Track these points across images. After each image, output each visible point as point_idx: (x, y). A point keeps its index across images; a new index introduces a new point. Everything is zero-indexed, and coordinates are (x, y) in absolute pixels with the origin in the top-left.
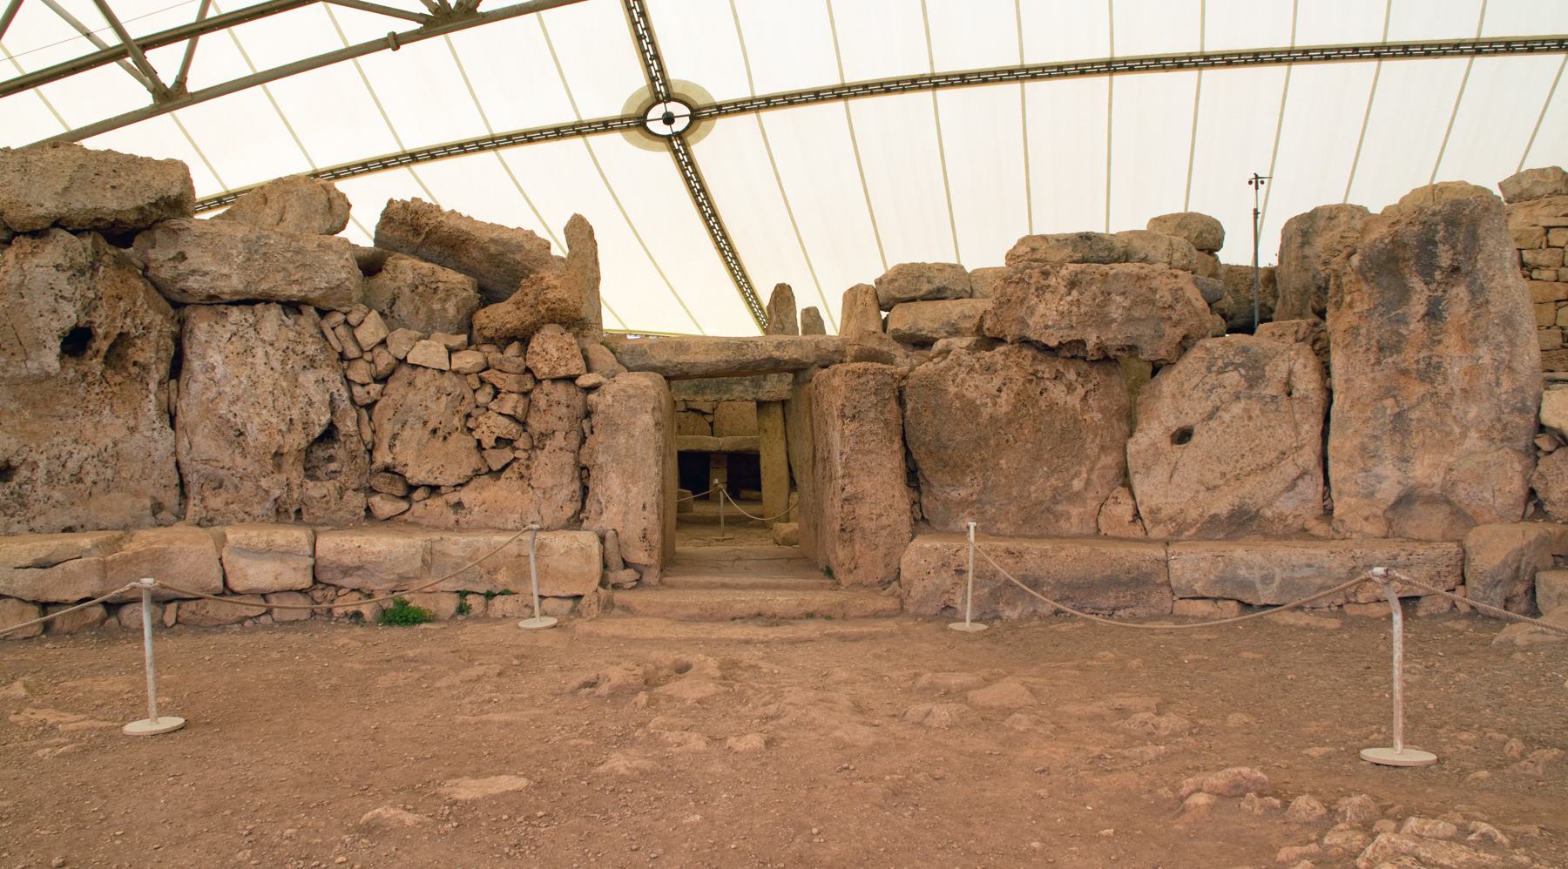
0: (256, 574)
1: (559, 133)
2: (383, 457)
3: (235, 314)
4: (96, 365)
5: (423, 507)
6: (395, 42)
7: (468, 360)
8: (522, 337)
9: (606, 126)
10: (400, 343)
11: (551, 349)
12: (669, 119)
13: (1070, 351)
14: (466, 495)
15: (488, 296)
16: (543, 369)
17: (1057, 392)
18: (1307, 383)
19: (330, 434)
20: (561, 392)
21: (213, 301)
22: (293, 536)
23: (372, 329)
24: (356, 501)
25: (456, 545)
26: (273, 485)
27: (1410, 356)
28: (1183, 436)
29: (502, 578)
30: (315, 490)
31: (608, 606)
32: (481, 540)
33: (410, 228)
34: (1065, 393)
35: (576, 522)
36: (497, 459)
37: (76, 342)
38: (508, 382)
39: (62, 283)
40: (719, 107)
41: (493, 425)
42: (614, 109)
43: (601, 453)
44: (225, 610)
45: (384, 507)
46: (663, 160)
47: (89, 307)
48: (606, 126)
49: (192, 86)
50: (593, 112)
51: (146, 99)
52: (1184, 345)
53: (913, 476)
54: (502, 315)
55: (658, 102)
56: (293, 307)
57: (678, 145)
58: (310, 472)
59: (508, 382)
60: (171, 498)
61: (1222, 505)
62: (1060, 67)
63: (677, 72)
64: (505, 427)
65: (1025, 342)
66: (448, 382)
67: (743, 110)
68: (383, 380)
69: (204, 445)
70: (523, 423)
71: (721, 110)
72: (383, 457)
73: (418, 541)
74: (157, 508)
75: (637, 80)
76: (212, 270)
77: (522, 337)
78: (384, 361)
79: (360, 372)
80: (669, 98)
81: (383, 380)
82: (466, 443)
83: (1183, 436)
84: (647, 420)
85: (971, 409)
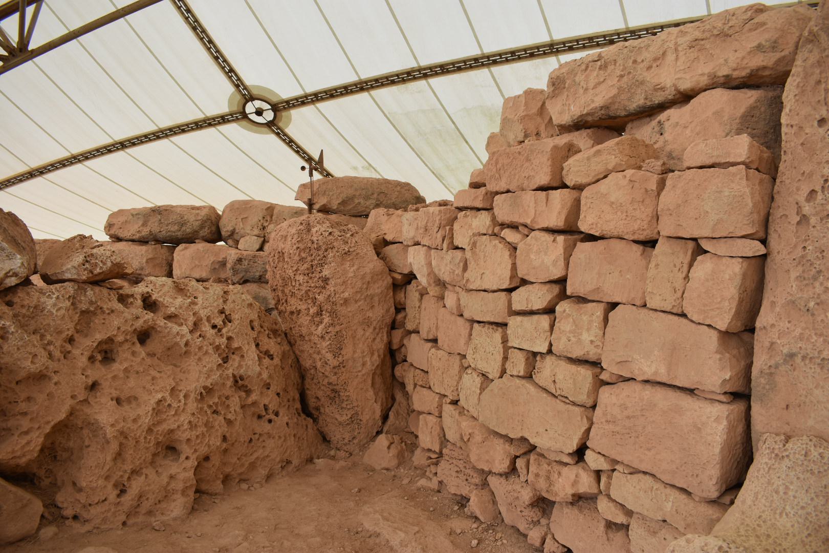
9: (223, 120)
12: (259, 112)
40: (287, 102)
48: (223, 120)
55: (247, 102)
62: (513, 53)
67: (303, 103)
80: (252, 98)
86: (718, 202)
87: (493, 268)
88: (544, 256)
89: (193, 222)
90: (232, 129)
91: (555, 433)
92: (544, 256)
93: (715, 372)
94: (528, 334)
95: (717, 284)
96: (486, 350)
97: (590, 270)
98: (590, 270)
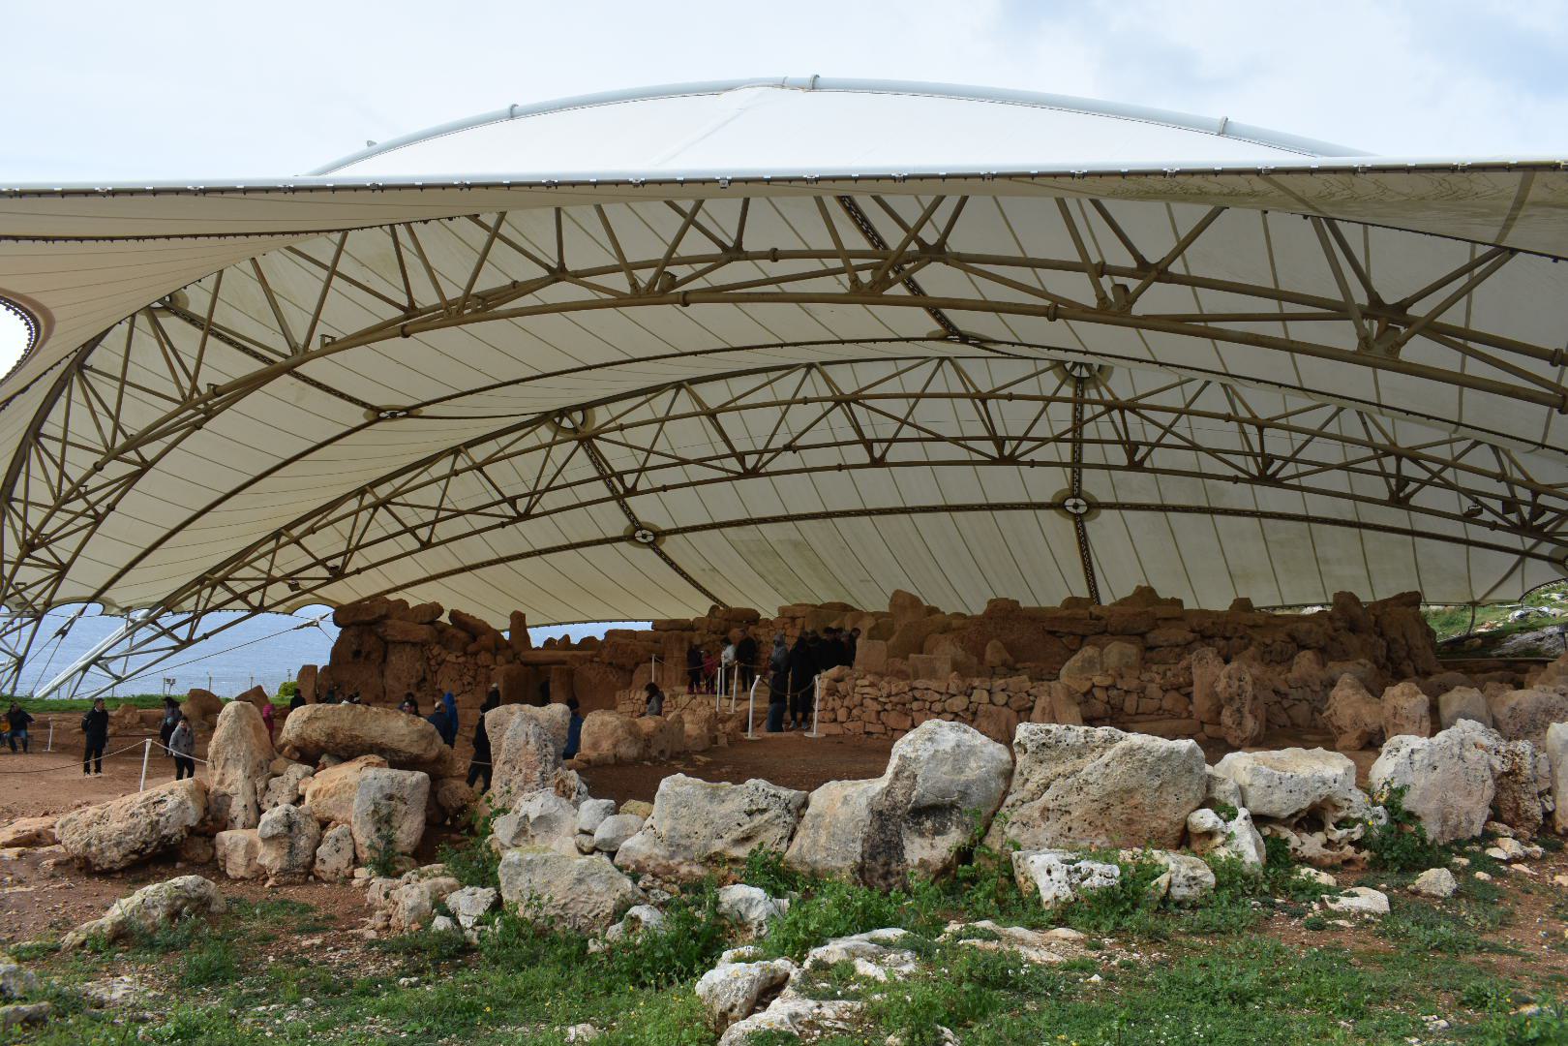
6: (503, 525)
8: (475, 654)
9: (618, 539)
10: (444, 654)
11: (484, 658)
12: (644, 536)
19: (424, 679)
37: (357, 654)
41: (467, 679)
42: (621, 533)
46: (650, 552)
48: (618, 539)
49: (434, 540)
51: (417, 545)
52: (637, 665)
54: (471, 648)
56: (414, 644)
69: (390, 681)
75: (627, 523)
90: (623, 546)
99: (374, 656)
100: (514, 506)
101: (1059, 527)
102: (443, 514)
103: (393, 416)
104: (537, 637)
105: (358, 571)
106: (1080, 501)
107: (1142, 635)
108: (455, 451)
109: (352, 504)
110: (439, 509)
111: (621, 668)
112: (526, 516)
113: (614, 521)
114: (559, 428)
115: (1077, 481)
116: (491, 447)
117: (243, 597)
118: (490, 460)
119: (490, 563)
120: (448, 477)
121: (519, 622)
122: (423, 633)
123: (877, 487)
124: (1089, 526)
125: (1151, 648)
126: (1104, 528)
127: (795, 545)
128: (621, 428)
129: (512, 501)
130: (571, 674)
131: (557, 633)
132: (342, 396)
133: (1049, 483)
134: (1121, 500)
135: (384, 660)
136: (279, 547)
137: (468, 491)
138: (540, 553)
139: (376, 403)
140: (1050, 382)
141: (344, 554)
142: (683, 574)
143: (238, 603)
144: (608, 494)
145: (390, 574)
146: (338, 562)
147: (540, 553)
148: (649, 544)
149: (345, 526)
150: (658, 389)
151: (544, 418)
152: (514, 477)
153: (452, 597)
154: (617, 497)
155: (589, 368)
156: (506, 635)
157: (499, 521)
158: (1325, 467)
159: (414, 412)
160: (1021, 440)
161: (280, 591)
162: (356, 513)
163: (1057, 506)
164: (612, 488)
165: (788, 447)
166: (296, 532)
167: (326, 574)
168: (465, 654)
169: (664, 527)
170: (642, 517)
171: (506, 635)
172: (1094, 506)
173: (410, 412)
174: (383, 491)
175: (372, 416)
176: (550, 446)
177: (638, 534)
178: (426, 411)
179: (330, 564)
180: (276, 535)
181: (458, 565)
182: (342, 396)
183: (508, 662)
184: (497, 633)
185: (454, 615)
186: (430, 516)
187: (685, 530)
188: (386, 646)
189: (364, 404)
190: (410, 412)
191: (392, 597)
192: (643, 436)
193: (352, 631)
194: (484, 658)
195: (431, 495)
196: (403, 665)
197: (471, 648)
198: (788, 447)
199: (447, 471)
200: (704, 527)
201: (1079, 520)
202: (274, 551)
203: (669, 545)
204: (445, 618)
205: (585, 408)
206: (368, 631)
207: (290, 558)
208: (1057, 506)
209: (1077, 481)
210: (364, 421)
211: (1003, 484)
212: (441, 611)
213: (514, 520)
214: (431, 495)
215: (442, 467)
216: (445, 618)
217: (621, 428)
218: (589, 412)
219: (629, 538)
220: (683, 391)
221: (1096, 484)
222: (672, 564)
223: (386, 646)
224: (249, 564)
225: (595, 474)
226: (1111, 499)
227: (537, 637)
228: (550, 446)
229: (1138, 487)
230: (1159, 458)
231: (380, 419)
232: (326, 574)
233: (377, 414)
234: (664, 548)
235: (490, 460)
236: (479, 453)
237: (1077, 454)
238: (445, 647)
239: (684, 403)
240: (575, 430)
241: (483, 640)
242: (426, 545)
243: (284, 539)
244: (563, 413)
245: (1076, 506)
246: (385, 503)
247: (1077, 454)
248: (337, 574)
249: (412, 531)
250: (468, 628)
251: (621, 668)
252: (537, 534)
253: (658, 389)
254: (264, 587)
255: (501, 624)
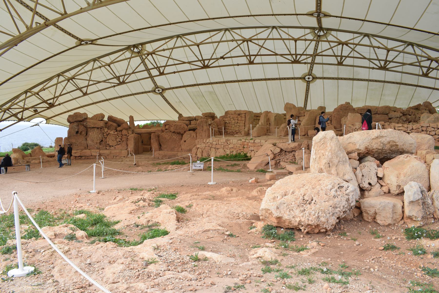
0: (94, 154)
1: (142, 93)
2: (107, 143)
3: (92, 129)
4: (79, 134)
5: (112, 148)
6: (114, 86)
7: (116, 133)
8: (121, 131)
9: (149, 92)
10: (109, 131)
11: (124, 132)
12: (159, 91)
13: (174, 132)
14: (116, 147)
15: (119, 126)
16: (123, 134)
17: (174, 136)
18: (195, 136)
19: (102, 141)
20: (125, 136)
21: (90, 128)
22: (98, 150)
23: (106, 130)
24: (105, 147)
25: (113, 152)
26: (96, 146)
27: (200, 134)
28: (185, 141)
29: (117, 155)
30: (100, 146)
31: (127, 157)
32: (115, 151)
33: (111, 118)
34: (175, 137)
35: (126, 149)
36: (119, 143)
37: (77, 132)
38: (120, 135)
39: (76, 127)
41: (118, 140)
42: (150, 90)
43: (129, 142)
44: (91, 157)
45: (108, 148)
47: (78, 129)
48: (149, 92)
49: (88, 93)
50: (147, 90)
51: (82, 94)
52: (185, 132)
53: (160, 145)
56: (98, 128)
57: (161, 94)
58: (100, 144)
59: (120, 135)
60: (86, 147)
61: (188, 148)
63: (158, 84)
64: (120, 140)
65: (171, 132)
66: (114, 135)
68: (107, 135)
69: (89, 142)
70: (121, 139)
71: (167, 89)
72: (107, 143)
73: (110, 151)
74: (85, 148)
75: (153, 86)
76: (90, 125)
77: (121, 131)
78: (107, 133)
79: (105, 134)
80: (158, 88)
81: (107, 135)
82: (115, 141)
83: (185, 141)
84: (133, 139)
85: (166, 138)
86: (243, 119)
87: (234, 122)
88: (236, 121)
89: (194, 118)
91: (237, 129)
92: (236, 121)
93: (244, 125)
94: (236, 125)
95: (244, 122)
96: (233, 126)
97: (239, 122)
98: (239, 122)
99: (83, 133)
100: (119, 80)
101: (302, 85)
102: (91, 83)
103: (87, 43)
104: (136, 123)
105: (59, 104)
106: (311, 77)
107: (387, 114)
108: (94, 60)
109: (55, 81)
110: (89, 80)
111: (179, 133)
112: (123, 83)
113: (148, 85)
114: (133, 52)
115: (311, 69)
116: (113, 57)
117: (15, 115)
118: (112, 63)
119: (103, 101)
120: (91, 70)
121: (132, 119)
122: (101, 124)
123: (256, 71)
124: (311, 85)
125: (390, 119)
126: (316, 86)
127: (210, 93)
128: (164, 50)
129: (118, 78)
130: (159, 136)
131: (142, 123)
132: (70, 34)
133: (301, 70)
134: (324, 76)
135: (87, 135)
136: (26, 98)
137: (101, 74)
138: (121, 97)
139: (82, 38)
140: (310, 37)
141: (53, 98)
142: (169, 103)
143: (13, 118)
144: (148, 76)
145: (73, 104)
146: (51, 101)
147: (121, 97)
148: (160, 93)
149: (52, 89)
150: (171, 37)
151: (128, 48)
152: (120, 68)
153: (109, 110)
154: (151, 77)
155: (170, 24)
156: (128, 123)
157: (113, 85)
158: (404, 64)
159: (94, 42)
160: (301, 55)
161: (27, 114)
162: (57, 84)
163: (303, 78)
164: (150, 74)
165: (222, 58)
166: (36, 90)
167: (48, 106)
168: (117, 131)
169: (166, 87)
170: (159, 84)
171: (128, 123)
172: (315, 78)
173: (92, 42)
174: (69, 75)
175: (79, 42)
176: (130, 58)
177: (157, 90)
178: (99, 42)
179: (49, 102)
180: (26, 92)
181: (92, 102)
182: (70, 34)
183: (132, 133)
184: (126, 122)
185: (110, 118)
186: (86, 83)
187: (173, 88)
188: (87, 129)
189: (77, 38)
190: (92, 42)
191: (81, 111)
192: (167, 53)
193: (75, 124)
194: (124, 132)
195: (86, 76)
196: (94, 135)
197: (119, 129)
198: (222, 58)
199: (91, 68)
200: (180, 87)
201: (308, 83)
202: (25, 100)
203: (167, 94)
204: (106, 119)
205: (142, 44)
206: (78, 123)
207: (32, 101)
208: (303, 78)
209: (311, 69)
210: (75, 45)
211: (288, 70)
212: (103, 116)
213: (119, 85)
214: (86, 76)
215: (89, 67)
216: (106, 119)
217: (164, 50)
218: (144, 46)
219: (154, 91)
220: (179, 38)
221: (317, 71)
222: (166, 100)
223: (87, 129)
224: (16, 104)
225: (145, 69)
226: (321, 76)
227: (136, 123)
228: (130, 58)
229: (332, 71)
230: (348, 61)
231: (81, 44)
232: (48, 106)
233: (81, 42)
234: (165, 95)
235: (112, 63)
236: (107, 60)
237: (313, 60)
238: (108, 129)
239: (180, 42)
240: (139, 52)
241: (124, 125)
242: (85, 94)
243: (29, 94)
244: (135, 46)
245: (309, 78)
246: (73, 78)
247: (313, 60)
248: (51, 106)
249: (80, 89)
250: (115, 123)
251: (179, 133)
252: (122, 90)
253: (171, 37)
254: (23, 111)
255: (127, 119)
